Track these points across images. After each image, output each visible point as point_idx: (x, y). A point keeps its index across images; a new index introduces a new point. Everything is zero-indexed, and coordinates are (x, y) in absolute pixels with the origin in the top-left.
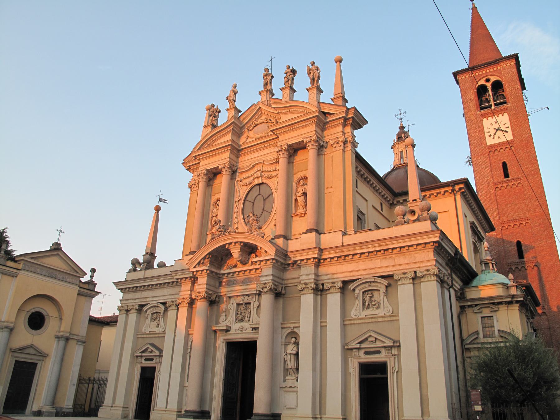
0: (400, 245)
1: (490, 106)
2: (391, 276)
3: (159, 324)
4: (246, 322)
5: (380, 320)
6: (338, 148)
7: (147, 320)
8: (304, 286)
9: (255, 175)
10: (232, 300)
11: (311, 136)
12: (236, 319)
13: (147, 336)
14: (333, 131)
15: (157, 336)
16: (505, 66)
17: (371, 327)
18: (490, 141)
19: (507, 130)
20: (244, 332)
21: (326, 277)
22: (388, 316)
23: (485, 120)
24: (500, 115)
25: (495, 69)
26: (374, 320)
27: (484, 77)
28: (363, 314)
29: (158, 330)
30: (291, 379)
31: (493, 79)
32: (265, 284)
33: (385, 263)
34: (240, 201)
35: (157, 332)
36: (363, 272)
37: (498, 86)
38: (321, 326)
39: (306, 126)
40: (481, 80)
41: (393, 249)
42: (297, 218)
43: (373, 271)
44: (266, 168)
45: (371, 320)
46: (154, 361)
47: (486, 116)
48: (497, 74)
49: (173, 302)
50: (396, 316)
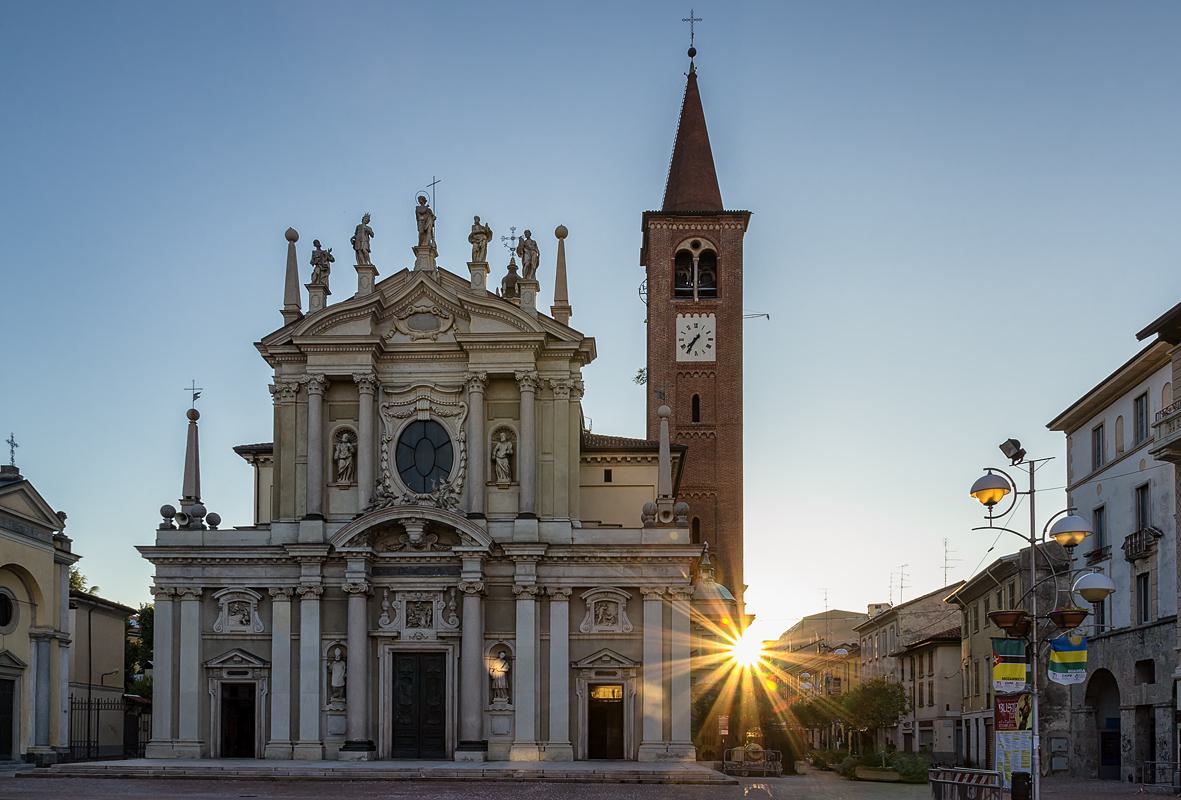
0: (653, 555)
1: (691, 293)
2: (638, 588)
3: (249, 621)
4: (424, 627)
5: (616, 637)
6: (562, 396)
7: (221, 613)
8: (522, 589)
9: (419, 405)
10: (398, 597)
11: (529, 369)
12: (407, 622)
13: (226, 637)
14: (552, 363)
15: (248, 638)
16: (727, 227)
17: (604, 645)
18: (682, 356)
19: (710, 343)
20: (422, 640)
21: (549, 580)
22: (626, 635)
23: (680, 315)
24: (704, 315)
25: (711, 227)
26: (608, 637)
27: (690, 237)
28: (596, 629)
29: (248, 629)
30: (500, 702)
31: (705, 245)
32: (471, 583)
33: (629, 572)
34: (390, 444)
35: (247, 633)
36: (600, 580)
37: (709, 258)
38: (541, 640)
39: (519, 350)
40: (685, 242)
41: (642, 557)
42: (496, 489)
43: (614, 580)
44: (436, 397)
45: (605, 637)
46: (249, 676)
47: (683, 310)
48: (713, 239)
49: (281, 589)
50: (635, 635)
